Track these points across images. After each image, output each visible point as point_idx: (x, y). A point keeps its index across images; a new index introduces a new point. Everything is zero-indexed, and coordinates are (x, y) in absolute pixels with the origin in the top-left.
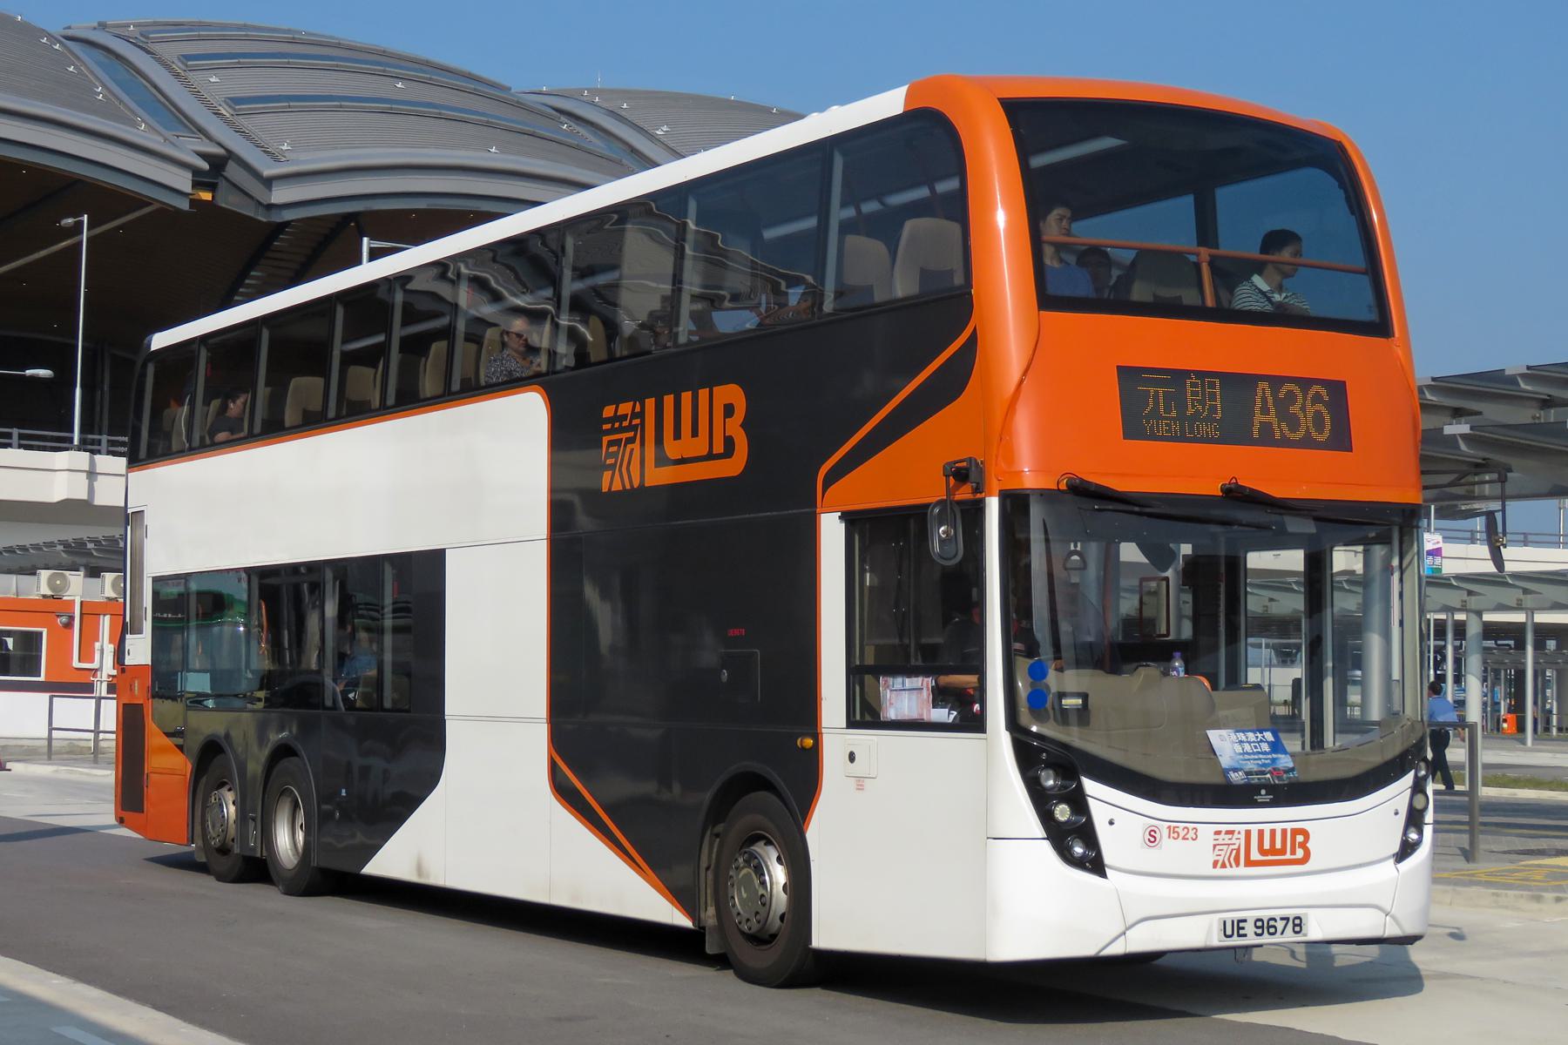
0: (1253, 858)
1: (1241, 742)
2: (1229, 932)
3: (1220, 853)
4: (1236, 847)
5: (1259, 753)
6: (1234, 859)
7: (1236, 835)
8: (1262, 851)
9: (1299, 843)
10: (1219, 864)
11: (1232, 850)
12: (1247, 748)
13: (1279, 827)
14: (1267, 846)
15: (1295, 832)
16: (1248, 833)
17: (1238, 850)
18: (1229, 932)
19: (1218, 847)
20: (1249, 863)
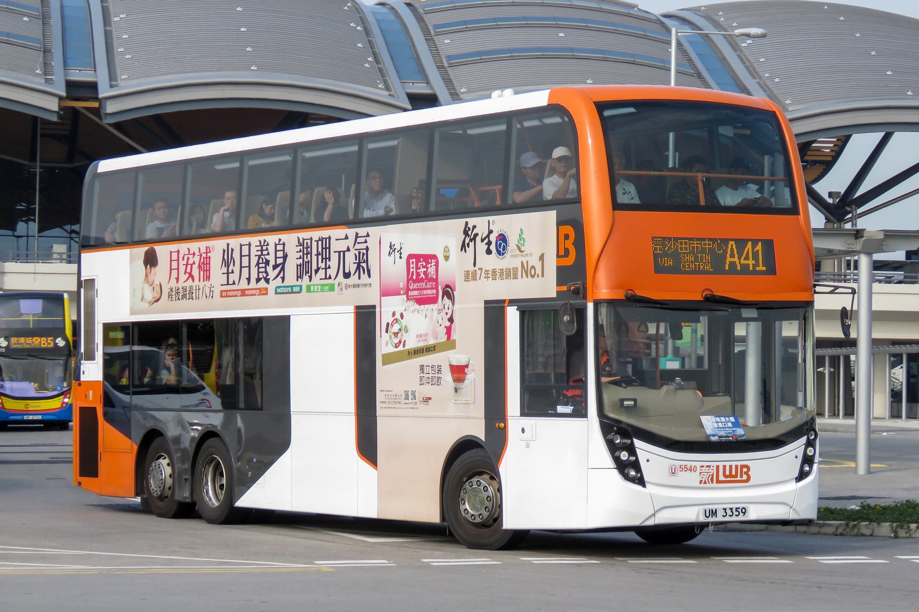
0: (720, 479)
1: (717, 422)
2: (708, 515)
3: (703, 476)
4: (711, 474)
5: (726, 427)
6: (711, 479)
7: (711, 468)
8: (725, 476)
9: (745, 472)
10: (703, 482)
11: (710, 475)
12: (720, 425)
13: (734, 464)
14: (727, 473)
15: (743, 467)
16: (718, 467)
17: (713, 475)
18: (708, 515)
19: (702, 474)
20: (718, 482)
